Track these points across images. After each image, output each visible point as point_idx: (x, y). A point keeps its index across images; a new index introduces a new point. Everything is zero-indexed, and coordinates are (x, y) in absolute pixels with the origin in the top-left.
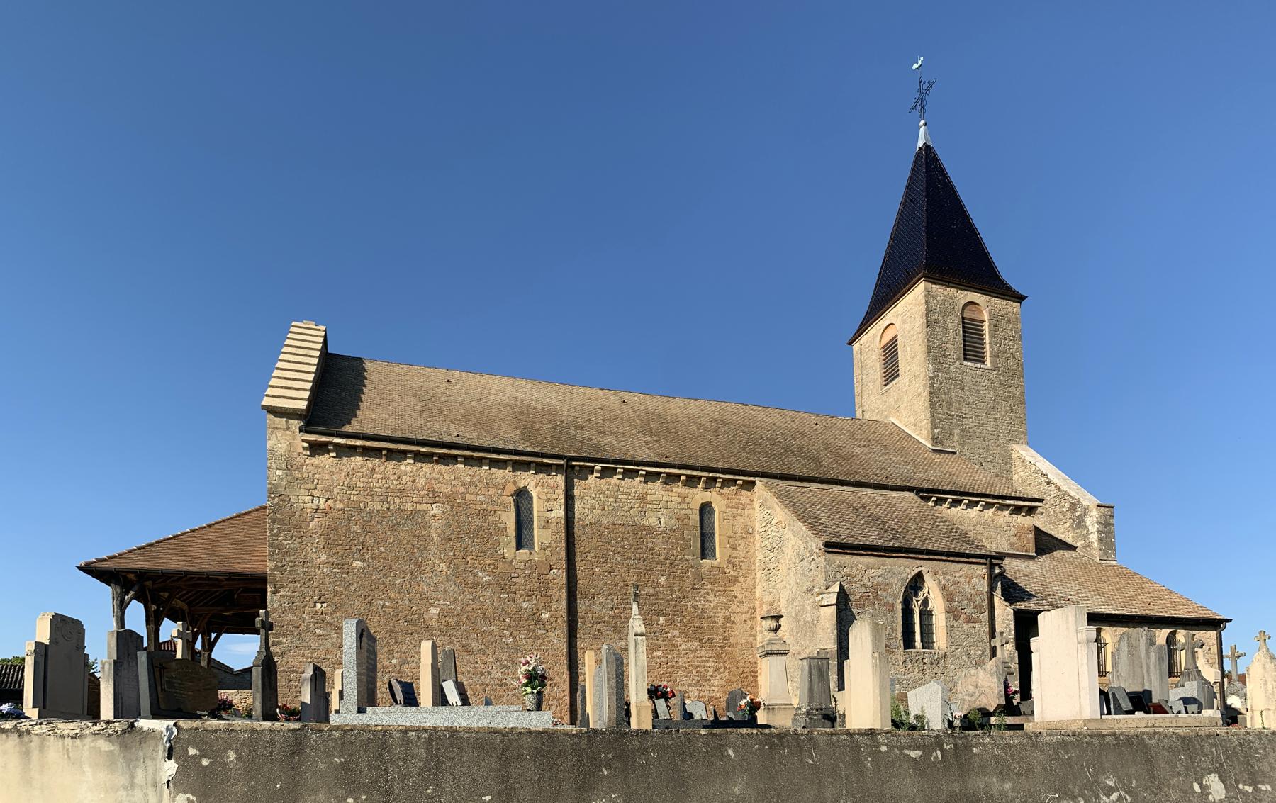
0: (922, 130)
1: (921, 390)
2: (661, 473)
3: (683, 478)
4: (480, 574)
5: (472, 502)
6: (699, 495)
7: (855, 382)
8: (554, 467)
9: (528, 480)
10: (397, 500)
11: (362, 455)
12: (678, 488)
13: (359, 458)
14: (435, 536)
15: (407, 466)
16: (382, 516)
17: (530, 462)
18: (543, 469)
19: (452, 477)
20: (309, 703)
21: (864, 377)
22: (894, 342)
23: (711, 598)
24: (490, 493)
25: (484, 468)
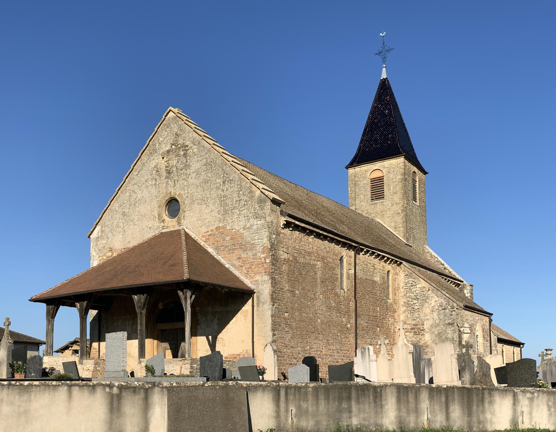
1: (400, 211)
2: (381, 255)
3: (398, 263)
4: (332, 302)
6: (389, 267)
7: (349, 190)
8: (335, 241)
10: (308, 258)
12: (382, 263)
13: (297, 232)
14: (319, 280)
15: (311, 239)
16: (305, 265)
17: (347, 243)
18: (350, 247)
19: (324, 248)
20: (97, 311)
22: (381, 179)
23: (390, 319)
24: (334, 258)
25: (333, 244)
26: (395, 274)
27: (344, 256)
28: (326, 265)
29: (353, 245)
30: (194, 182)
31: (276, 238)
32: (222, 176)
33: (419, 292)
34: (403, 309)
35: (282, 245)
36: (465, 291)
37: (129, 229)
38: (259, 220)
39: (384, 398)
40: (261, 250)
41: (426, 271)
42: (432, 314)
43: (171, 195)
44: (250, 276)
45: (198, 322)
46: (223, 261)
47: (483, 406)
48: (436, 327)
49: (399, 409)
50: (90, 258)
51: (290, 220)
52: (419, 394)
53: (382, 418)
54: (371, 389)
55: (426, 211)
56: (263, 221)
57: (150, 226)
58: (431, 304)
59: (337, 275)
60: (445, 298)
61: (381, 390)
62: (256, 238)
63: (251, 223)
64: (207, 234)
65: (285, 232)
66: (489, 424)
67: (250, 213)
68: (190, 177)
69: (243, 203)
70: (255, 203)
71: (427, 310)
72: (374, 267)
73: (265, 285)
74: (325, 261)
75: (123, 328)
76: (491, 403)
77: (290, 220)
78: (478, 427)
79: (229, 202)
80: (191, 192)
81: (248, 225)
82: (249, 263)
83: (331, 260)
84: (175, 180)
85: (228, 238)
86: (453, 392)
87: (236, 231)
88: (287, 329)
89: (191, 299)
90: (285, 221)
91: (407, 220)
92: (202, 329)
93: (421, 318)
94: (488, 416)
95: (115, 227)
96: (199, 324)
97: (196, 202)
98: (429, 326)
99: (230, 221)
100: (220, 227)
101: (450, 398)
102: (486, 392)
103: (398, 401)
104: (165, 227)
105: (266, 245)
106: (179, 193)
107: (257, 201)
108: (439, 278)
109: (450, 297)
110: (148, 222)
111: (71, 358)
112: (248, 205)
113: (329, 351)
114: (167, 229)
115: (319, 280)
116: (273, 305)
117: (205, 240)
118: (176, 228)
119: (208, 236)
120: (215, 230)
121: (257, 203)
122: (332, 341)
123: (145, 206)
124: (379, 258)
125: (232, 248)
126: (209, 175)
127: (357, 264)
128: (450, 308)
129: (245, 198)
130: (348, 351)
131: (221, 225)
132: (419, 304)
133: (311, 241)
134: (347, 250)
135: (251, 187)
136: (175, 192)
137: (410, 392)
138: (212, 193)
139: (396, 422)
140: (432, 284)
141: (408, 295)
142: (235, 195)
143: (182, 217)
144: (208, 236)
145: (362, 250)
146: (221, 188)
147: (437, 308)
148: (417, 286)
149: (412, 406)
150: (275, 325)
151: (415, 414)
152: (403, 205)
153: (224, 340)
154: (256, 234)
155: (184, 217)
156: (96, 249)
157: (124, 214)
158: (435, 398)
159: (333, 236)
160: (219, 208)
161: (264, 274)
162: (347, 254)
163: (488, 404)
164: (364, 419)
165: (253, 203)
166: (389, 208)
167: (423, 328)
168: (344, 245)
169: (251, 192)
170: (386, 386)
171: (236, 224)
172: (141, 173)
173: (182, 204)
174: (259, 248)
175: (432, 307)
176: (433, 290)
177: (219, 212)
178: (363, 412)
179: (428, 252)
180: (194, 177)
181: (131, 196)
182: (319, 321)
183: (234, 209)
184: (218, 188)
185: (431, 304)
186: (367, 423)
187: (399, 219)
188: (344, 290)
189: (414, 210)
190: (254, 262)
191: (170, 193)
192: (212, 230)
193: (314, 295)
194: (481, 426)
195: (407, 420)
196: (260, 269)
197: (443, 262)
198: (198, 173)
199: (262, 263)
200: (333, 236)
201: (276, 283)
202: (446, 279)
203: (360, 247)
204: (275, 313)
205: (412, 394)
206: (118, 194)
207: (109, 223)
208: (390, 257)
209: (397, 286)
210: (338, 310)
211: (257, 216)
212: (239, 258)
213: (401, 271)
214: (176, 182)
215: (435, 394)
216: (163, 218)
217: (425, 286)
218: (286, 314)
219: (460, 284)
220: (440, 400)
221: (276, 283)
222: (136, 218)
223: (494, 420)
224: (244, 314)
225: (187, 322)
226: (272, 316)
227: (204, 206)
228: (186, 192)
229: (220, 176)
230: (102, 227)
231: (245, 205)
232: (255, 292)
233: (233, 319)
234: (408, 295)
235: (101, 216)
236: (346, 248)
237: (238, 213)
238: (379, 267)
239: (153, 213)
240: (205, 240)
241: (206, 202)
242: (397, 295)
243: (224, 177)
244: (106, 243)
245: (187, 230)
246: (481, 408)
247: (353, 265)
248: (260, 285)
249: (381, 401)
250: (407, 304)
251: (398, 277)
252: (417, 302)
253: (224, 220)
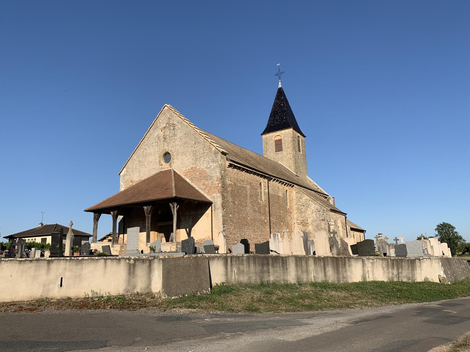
0: (280, 83)
1: (292, 157)
2: (282, 181)
3: (292, 185)
4: (256, 208)
5: (254, 186)
6: (286, 188)
8: (257, 174)
9: (262, 180)
11: (237, 169)
12: (283, 186)
13: (236, 170)
15: (243, 173)
16: (240, 187)
17: (263, 175)
18: (265, 177)
21: (267, 147)
26: (290, 192)
27: (262, 182)
28: (252, 187)
29: (267, 176)
30: (179, 144)
31: (224, 172)
32: (194, 140)
33: (304, 202)
34: (295, 211)
35: (228, 177)
36: (330, 201)
37: (142, 169)
38: (215, 163)
39: (288, 264)
40: (216, 179)
41: (308, 190)
42: (312, 214)
43: (166, 150)
44: (210, 194)
46: (195, 186)
47: (345, 267)
48: (315, 222)
49: (297, 271)
50: (119, 187)
51: (232, 163)
52: (308, 261)
53: (287, 276)
54: (280, 258)
55: (306, 157)
56: (217, 164)
57: (154, 168)
58: (311, 208)
59: (259, 192)
60: (319, 205)
61: (286, 259)
62: (213, 173)
63: (210, 165)
64: (186, 171)
65: (229, 169)
66: (349, 279)
67: (210, 160)
68: (176, 141)
69: (206, 154)
70: (212, 154)
71: (309, 212)
72: (278, 188)
73: (218, 199)
74: (252, 185)
76: (350, 266)
77: (232, 163)
78: (343, 281)
79: (198, 154)
80: (177, 149)
81: (209, 166)
82: (209, 187)
83: (255, 185)
84: (168, 143)
85: (198, 173)
86: (328, 260)
87: (202, 169)
88: (231, 224)
89: (177, 207)
90: (229, 163)
91: (296, 162)
93: (306, 216)
94: (349, 274)
95: (134, 169)
97: (180, 154)
98: (311, 221)
99: (199, 164)
100: (193, 167)
101: (326, 263)
102: (347, 260)
103: (296, 266)
104: (163, 168)
105: (218, 177)
106: (171, 150)
107: (214, 153)
108: (315, 194)
109: (322, 204)
110: (153, 165)
112: (209, 155)
113: (255, 236)
114: (163, 169)
115: (248, 195)
116: (223, 210)
117: (185, 175)
118: (169, 169)
119: (187, 172)
120: (190, 169)
121: (214, 154)
122: (257, 230)
123: (151, 157)
124: (281, 183)
125: (200, 179)
126: (187, 139)
127: (269, 186)
128: (322, 211)
129: (207, 151)
130: (266, 235)
131: (194, 166)
132: (304, 208)
133: (244, 174)
134: (264, 179)
135: (210, 146)
136: (168, 149)
137: (303, 260)
138: (189, 149)
139: (296, 278)
140: (311, 197)
141: (298, 203)
142: (201, 150)
143: (172, 163)
144: (187, 172)
145: (272, 179)
146: (194, 146)
147: (315, 211)
148: (303, 198)
149: (304, 268)
150: (224, 221)
151: (306, 273)
152: (293, 154)
154: (213, 171)
155: (173, 162)
156: (123, 181)
157: (140, 161)
158: (317, 263)
159: (255, 171)
160: (193, 157)
161: (218, 193)
162: (264, 181)
163: (348, 266)
164: (277, 277)
165: (211, 154)
166: (286, 156)
167: (308, 222)
168: (262, 176)
169: (210, 148)
170: (289, 256)
171: (202, 165)
172: (149, 139)
173: (172, 155)
174: (215, 179)
175: (312, 210)
176: (312, 201)
177: (192, 160)
178: (276, 273)
179: (308, 180)
180: (179, 141)
181: (143, 151)
182: (249, 218)
183: (201, 158)
184: (192, 146)
185: (311, 208)
186: (278, 279)
187: (292, 162)
188: (263, 201)
189: (299, 157)
190: (212, 186)
191: (166, 149)
192: (189, 169)
193: (246, 204)
194: (345, 280)
195: (302, 277)
196: (215, 190)
197: (317, 185)
198: (181, 139)
199: (217, 187)
200: (255, 171)
201: (224, 198)
202: (319, 194)
203: (271, 177)
204: (224, 214)
205: (304, 261)
206: (137, 151)
207: (131, 167)
208: (287, 182)
209: (291, 199)
210: (260, 212)
211: (213, 161)
212: (204, 184)
213: (293, 190)
214: (169, 144)
215: (317, 261)
216: (161, 163)
217: (307, 198)
218: (230, 215)
219: (327, 197)
220: (321, 265)
221: (224, 198)
222: (146, 164)
223: (352, 276)
224: (207, 215)
225: (174, 221)
226: (223, 216)
227: (184, 156)
228: (174, 149)
229: (193, 140)
230: (127, 169)
231: (207, 155)
232: (213, 203)
233: (200, 218)
234: (298, 203)
235: (126, 163)
236: (263, 178)
237: (203, 159)
238: (281, 188)
239: (156, 161)
240: (185, 175)
241: (185, 154)
242: (292, 203)
243: (195, 140)
244: (129, 178)
245: (175, 170)
246: (344, 269)
247: (267, 187)
248: (216, 199)
249: (286, 265)
250: (298, 209)
251: (292, 193)
252: (303, 207)
253: (195, 164)
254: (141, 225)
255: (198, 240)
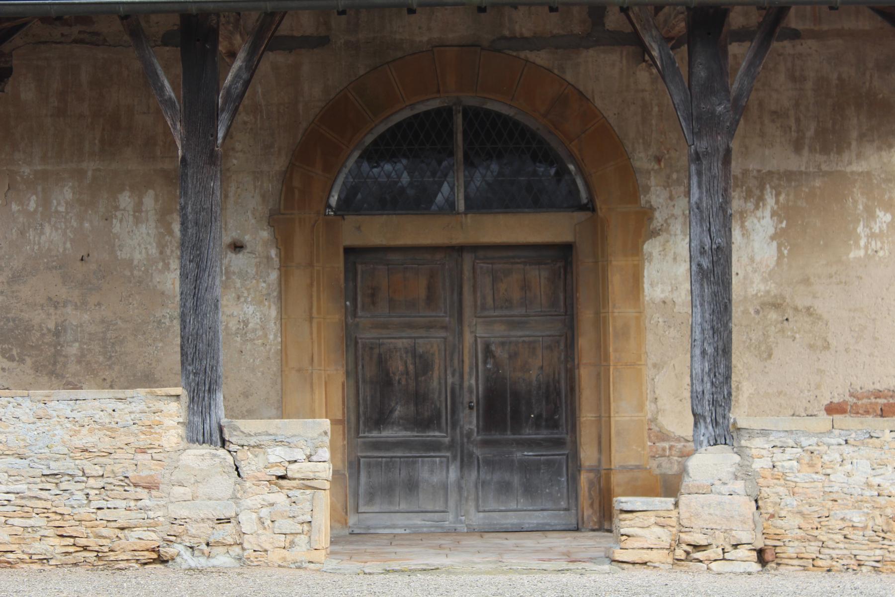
45: (651, 219)
75: (87, 225)
92: (675, 259)
96: (655, 234)
111: (120, 405)
153: (820, 318)
254: (138, 221)
255: (852, 400)
